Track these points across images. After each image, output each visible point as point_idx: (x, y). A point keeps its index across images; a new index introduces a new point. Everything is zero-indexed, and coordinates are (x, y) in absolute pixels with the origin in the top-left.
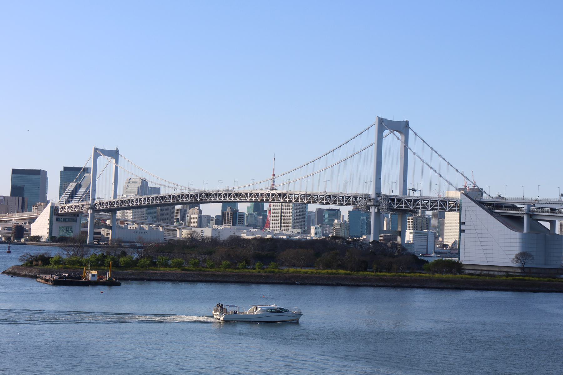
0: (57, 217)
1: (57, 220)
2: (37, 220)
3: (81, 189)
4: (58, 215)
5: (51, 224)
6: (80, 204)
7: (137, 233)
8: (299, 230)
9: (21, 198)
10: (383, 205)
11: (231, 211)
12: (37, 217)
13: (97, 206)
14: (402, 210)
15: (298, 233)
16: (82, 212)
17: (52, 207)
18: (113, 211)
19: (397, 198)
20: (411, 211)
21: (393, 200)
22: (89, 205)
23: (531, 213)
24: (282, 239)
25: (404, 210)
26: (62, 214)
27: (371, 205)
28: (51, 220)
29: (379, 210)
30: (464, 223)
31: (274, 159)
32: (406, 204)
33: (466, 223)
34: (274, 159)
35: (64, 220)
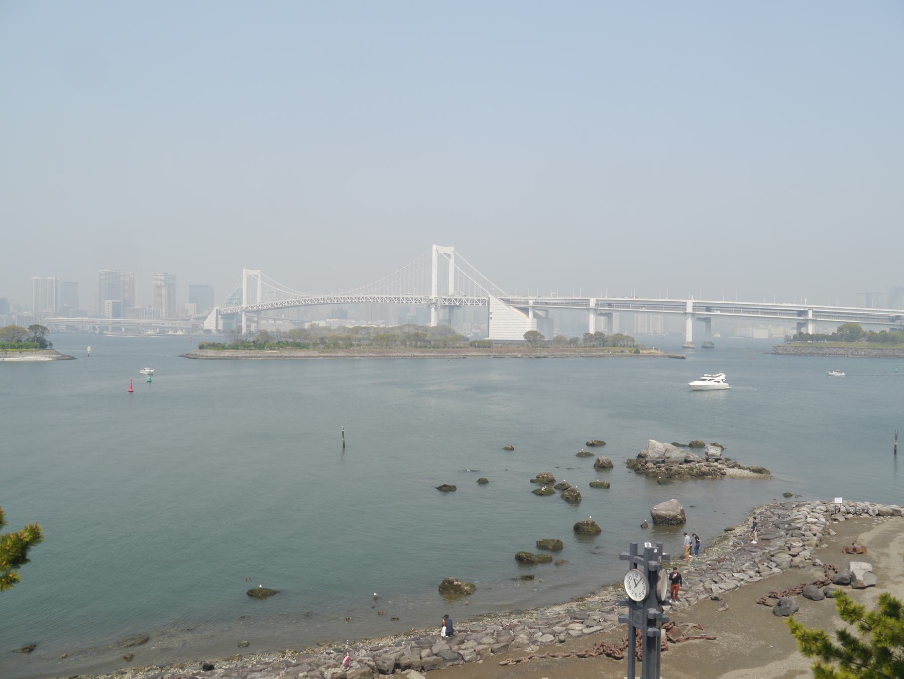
1: (221, 318)
2: (207, 319)
5: (217, 321)
6: (236, 307)
8: (384, 321)
9: (196, 304)
12: (207, 317)
15: (383, 322)
16: (238, 313)
17: (217, 310)
18: (258, 312)
20: (457, 306)
21: (445, 299)
22: (242, 308)
23: (533, 306)
24: (373, 327)
26: (224, 315)
27: (431, 303)
28: (217, 318)
29: (436, 306)
30: (491, 313)
32: (454, 301)
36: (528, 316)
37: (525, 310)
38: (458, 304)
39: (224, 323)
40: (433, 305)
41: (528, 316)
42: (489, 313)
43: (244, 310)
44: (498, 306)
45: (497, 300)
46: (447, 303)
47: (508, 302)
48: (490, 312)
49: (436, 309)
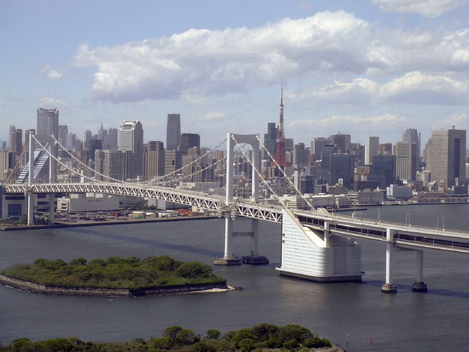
0: (8, 196)
3: (44, 156)
4: (7, 194)
7: (91, 201)
10: (233, 214)
11: (200, 166)
13: (35, 189)
14: (246, 217)
19: (243, 206)
21: (241, 208)
23: (328, 230)
25: (248, 217)
31: (282, 88)
33: (285, 235)
34: (282, 88)
35: (13, 198)
36: (324, 241)
37: (320, 233)
38: (253, 216)
39: (9, 205)
40: (227, 213)
41: (324, 241)
42: (282, 235)
43: (30, 191)
44: (290, 226)
45: (290, 219)
46: (242, 214)
47: (302, 220)
48: (283, 233)
49: (230, 219)
